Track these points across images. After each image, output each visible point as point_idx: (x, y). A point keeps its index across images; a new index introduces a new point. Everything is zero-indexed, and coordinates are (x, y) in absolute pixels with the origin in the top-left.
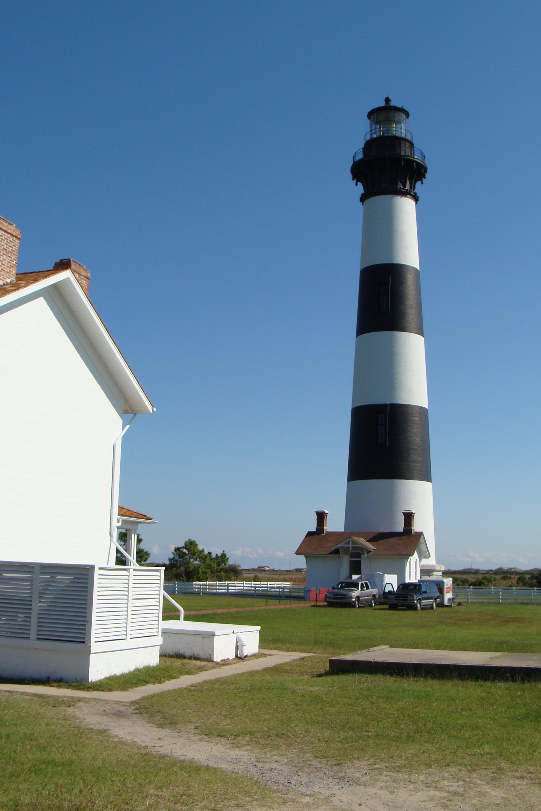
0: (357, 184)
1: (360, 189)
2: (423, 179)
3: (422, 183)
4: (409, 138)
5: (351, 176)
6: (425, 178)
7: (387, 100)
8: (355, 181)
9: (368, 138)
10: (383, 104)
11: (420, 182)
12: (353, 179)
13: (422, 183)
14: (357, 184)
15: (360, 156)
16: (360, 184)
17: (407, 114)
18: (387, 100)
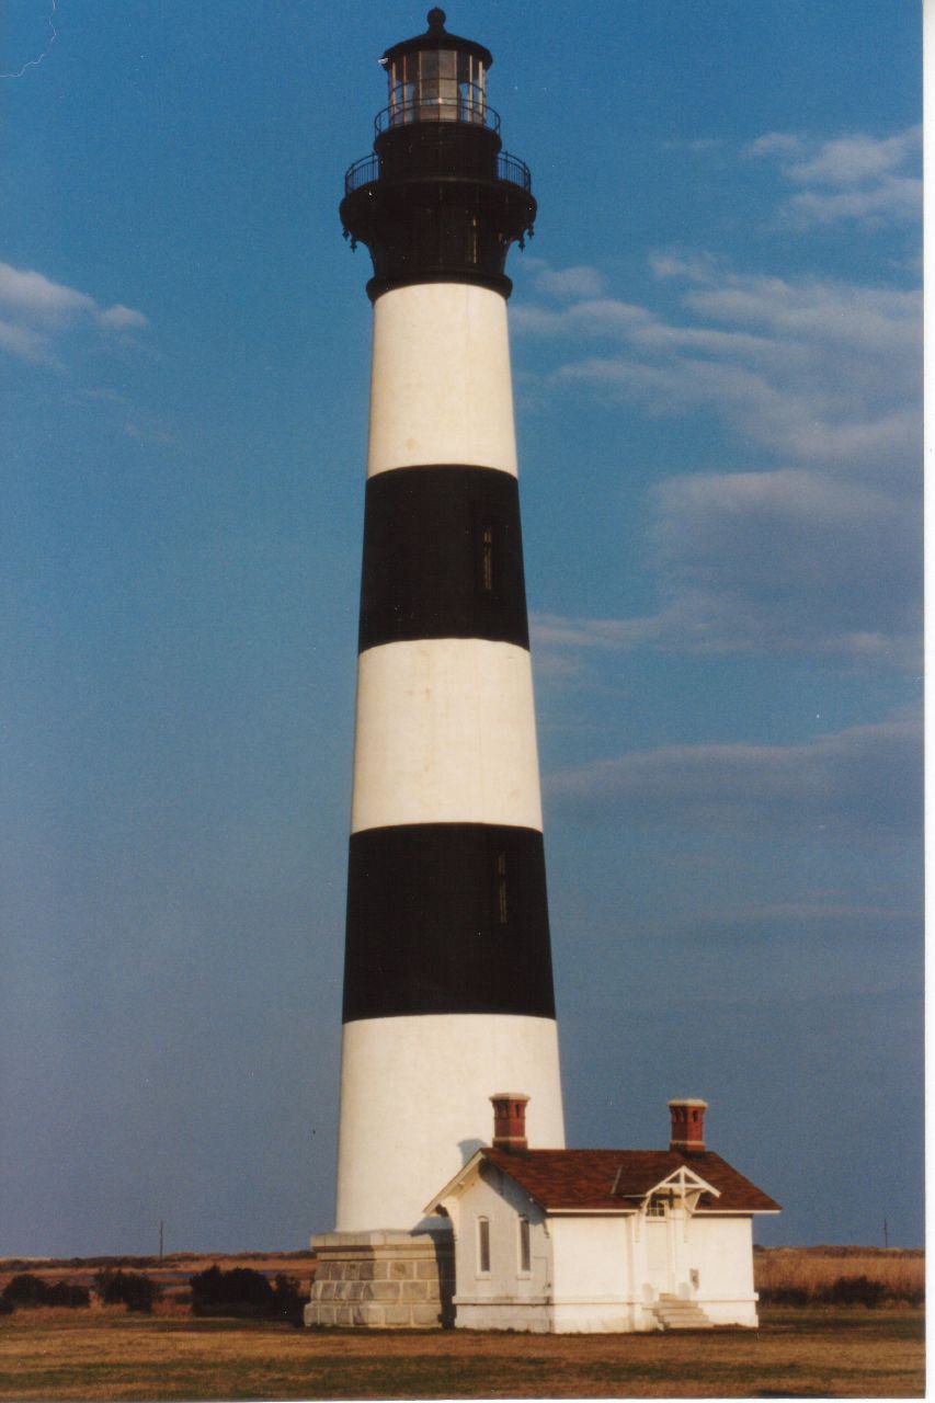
0: (354, 247)
1: (361, 262)
2: (526, 236)
3: (522, 246)
4: (491, 125)
5: (340, 227)
6: (531, 234)
7: (436, 17)
8: (350, 237)
9: (385, 126)
10: (421, 28)
11: (515, 245)
12: (346, 235)
13: (522, 246)
14: (354, 247)
15: (369, 174)
16: (362, 248)
17: (484, 56)
18: (436, 17)
